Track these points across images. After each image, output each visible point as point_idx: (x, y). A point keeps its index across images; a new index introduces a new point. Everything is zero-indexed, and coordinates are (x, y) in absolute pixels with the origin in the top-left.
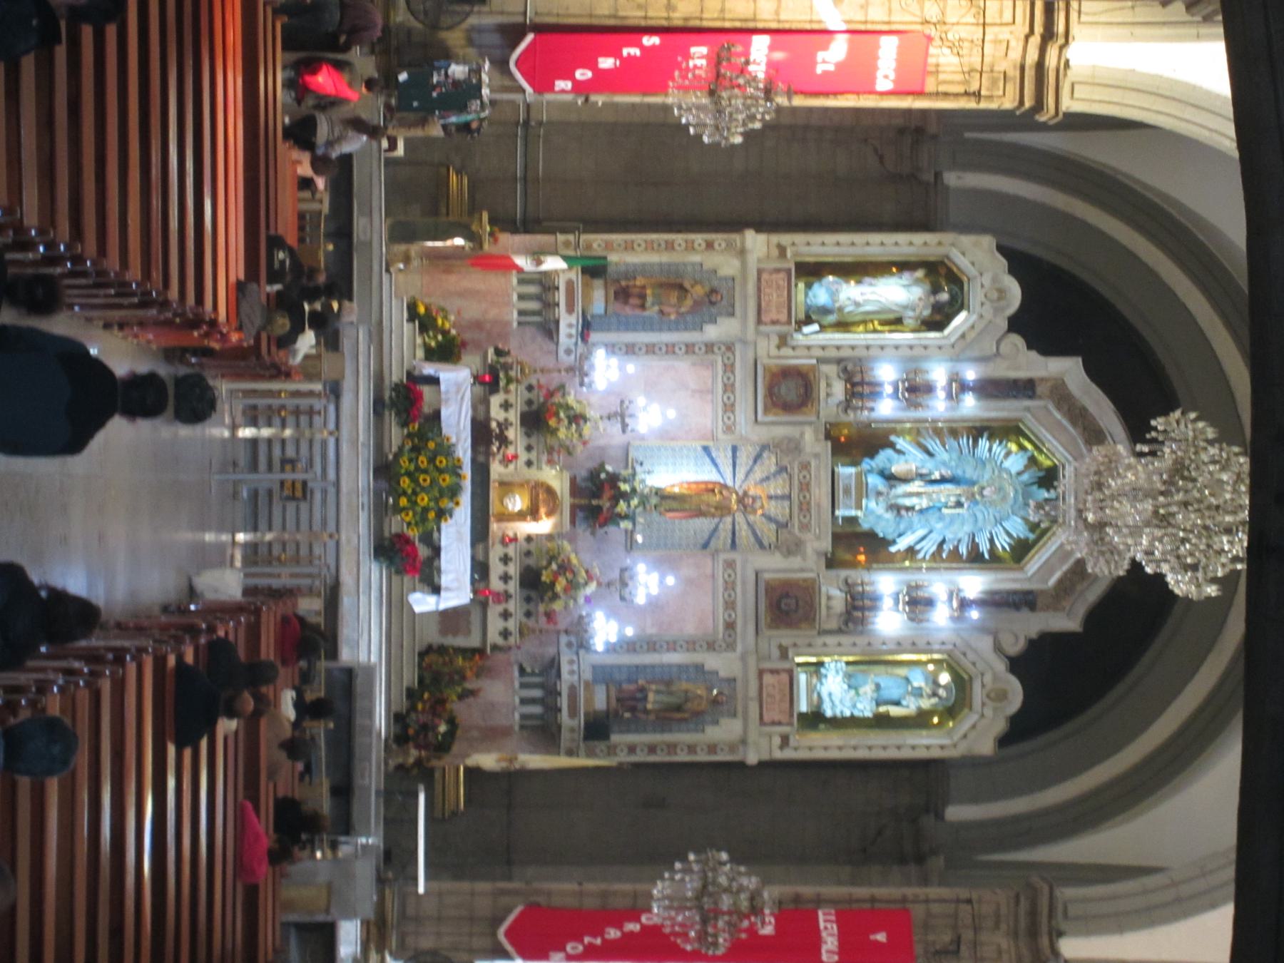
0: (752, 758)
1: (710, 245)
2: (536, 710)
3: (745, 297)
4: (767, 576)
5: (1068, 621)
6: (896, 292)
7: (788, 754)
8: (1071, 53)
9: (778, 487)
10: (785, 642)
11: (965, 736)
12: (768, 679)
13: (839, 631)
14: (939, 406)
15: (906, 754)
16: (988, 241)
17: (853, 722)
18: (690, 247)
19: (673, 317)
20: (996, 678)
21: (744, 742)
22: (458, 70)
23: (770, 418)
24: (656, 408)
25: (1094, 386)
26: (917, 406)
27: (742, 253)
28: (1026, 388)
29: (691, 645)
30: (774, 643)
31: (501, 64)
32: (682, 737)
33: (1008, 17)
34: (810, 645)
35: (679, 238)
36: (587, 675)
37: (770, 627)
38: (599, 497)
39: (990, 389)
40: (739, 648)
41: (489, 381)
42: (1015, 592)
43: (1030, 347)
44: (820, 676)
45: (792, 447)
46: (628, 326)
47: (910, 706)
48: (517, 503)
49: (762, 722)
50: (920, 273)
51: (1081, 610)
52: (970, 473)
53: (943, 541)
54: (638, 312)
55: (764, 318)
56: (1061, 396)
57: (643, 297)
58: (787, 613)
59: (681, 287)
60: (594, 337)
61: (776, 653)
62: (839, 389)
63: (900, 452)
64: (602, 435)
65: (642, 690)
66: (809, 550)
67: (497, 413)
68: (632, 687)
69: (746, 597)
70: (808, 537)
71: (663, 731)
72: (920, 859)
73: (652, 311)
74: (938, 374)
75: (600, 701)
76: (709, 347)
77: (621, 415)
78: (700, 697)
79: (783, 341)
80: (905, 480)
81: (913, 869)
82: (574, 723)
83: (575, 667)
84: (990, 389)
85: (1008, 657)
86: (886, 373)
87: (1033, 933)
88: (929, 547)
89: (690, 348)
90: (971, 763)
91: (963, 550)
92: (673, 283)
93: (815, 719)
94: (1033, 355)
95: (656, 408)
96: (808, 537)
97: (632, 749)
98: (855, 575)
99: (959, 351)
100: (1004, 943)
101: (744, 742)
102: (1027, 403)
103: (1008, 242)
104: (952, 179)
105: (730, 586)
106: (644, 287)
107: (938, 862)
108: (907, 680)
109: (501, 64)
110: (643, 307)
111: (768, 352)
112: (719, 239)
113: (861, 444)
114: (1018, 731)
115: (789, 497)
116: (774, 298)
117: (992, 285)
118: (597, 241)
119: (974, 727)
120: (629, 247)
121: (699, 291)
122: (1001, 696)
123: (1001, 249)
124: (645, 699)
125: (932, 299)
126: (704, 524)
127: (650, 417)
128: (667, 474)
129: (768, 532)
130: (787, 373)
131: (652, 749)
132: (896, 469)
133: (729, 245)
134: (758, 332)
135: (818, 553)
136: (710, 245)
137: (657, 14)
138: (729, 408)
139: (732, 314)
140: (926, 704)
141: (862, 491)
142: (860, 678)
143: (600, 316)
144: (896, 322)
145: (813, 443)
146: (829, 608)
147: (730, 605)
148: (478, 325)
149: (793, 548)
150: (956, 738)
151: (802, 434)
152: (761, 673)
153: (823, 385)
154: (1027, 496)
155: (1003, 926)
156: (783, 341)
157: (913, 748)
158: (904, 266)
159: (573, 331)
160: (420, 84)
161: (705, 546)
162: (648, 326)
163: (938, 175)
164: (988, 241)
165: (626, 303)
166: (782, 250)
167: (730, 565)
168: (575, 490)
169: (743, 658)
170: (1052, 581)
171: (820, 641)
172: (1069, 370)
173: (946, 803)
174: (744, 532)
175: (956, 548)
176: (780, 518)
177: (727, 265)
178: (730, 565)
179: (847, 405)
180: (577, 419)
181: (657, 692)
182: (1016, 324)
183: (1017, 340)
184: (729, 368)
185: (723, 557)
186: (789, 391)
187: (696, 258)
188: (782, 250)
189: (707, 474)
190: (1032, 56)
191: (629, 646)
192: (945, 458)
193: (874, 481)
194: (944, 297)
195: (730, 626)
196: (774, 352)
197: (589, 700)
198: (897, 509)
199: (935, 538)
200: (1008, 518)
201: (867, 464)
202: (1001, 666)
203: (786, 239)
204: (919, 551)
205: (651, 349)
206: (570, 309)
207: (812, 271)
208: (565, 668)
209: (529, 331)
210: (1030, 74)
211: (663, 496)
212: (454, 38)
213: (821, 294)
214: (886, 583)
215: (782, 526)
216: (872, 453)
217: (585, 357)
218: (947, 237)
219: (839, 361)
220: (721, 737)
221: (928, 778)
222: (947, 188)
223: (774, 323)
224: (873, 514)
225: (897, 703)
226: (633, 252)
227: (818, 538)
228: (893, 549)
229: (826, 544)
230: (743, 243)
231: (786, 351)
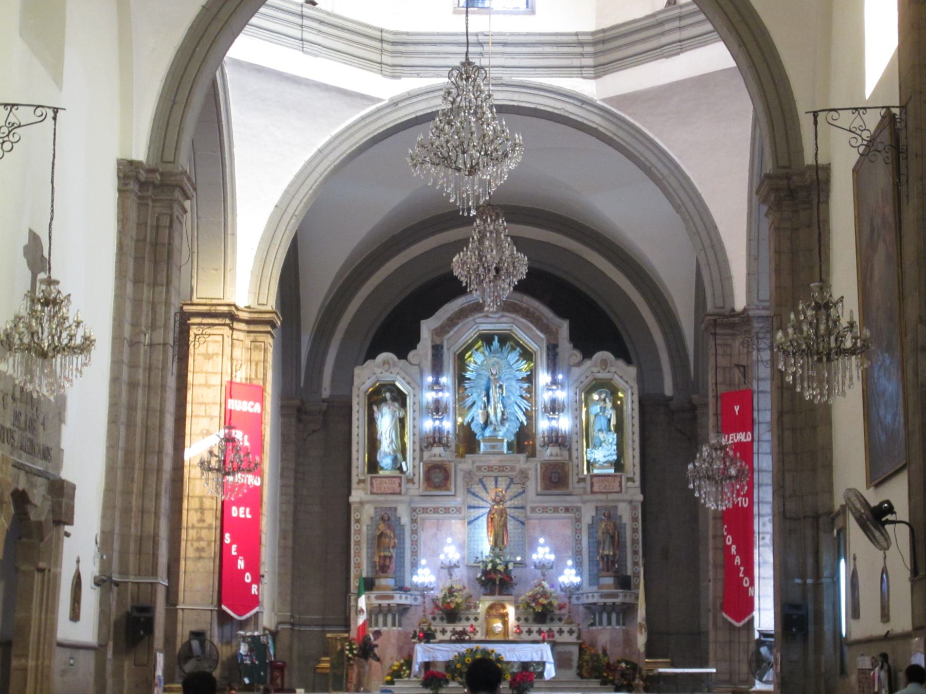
0: (640, 497)
1: (358, 521)
2: (614, 616)
3: (386, 501)
4: (539, 489)
5: (564, 328)
6: (385, 422)
7: (637, 478)
8: (241, 305)
9: (491, 484)
10: (575, 479)
11: (627, 382)
12: (596, 489)
13: (570, 450)
14: (447, 396)
15: (636, 414)
16: (357, 371)
18: (359, 532)
19: (396, 541)
20: (595, 366)
21: (631, 502)
22: (244, 649)
24: (447, 549)
25: (437, 314)
26: (446, 408)
27: (362, 503)
28: (437, 350)
29: (578, 531)
30: (577, 485)
31: (242, 625)
34: (577, 466)
35: (353, 538)
36: (595, 588)
37: (567, 488)
38: (496, 580)
39: (437, 370)
40: (579, 505)
41: (428, 637)
42: (548, 355)
44: (595, 461)
45: (469, 475)
46: (402, 566)
47: (611, 413)
48: (498, 625)
49: (621, 492)
50: (375, 408)
51: (557, 320)
52: (483, 382)
53: (521, 396)
54: (393, 560)
55: (398, 491)
56: (441, 331)
57: (385, 557)
58: (559, 478)
59: (381, 535)
60: (407, 585)
61: (582, 485)
62: (437, 450)
63: (473, 420)
64: (461, 576)
65: (602, 558)
67: (447, 636)
68: (601, 564)
69: (551, 501)
70: (518, 467)
71: (625, 547)
72: (693, 408)
73: (393, 552)
74: (429, 396)
75: (609, 581)
76: (414, 521)
77: (450, 568)
78: (606, 526)
79: (410, 481)
80: (488, 415)
81: (698, 412)
82: (621, 595)
83: (590, 595)
84: (437, 370)
85: (584, 358)
86: (428, 425)
88: (524, 404)
89: (414, 532)
90: (641, 379)
91: (526, 385)
92: (378, 540)
93: (618, 465)
94: (419, 346)
95: (447, 549)
96: (518, 467)
97: (635, 564)
98: (539, 441)
99: (418, 386)
101: (631, 502)
102: (445, 349)
104: (326, 393)
105: (545, 510)
106: (380, 557)
107: (695, 397)
108: (596, 415)
109: (242, 625)
110: (391, 557)
111: (417, 489)
112: (353, 517)
113: (468, 441)
114: (623, 354)
116: (387, 486)
118: (354, 583)
119: (621, 377)
120: (358, 566)
121: (382, 527)
122: (604, 363)
124: (607, 556)
125: (390, 402)
126: (511, 524)
127: (451, 553)
128: (484, 546)
129: (515, 489)
130: (428, 479)
131: (635, 553)
132: (481, 420)
133: (357, 510)
134: (406, 494)
135: (527, 461)
137: (213, 535)
138: (447, 510)
139: (396, 509)
140: (609, 405)
141: (493, 439)
142: (596, 440)
143: (396, 581)
144: (402, 421)
145: (467, 463)
146: (557, 455)
147: (556, 510)
148: (400, 649)
149: (524, 475)
150: (627, 387)
151: (461, 470)
152: (592, 492)
153: (434, 459)
154: (496, 352)
155: (729, 342)
156: (410, 481)
157: (633, 410)
159: (404, 596)
160: (251, 671)
161: (523, 523)
162: (401, 556)
163: (323, 401)
165: (388, 567)
166: (360, 481)
167: (533, 510)
168: (492, 593)
169: (584, 502)
170: (542, 336)
171: (575, 460)
172: (427, 327)
173: (663, 395)
174: (516, 502)
175: (525, 389)
176: (508, 482)
177: (368, 512)
178: (533, 510)
179: (446, 446)
180: (451, 591)
181: (603, 549)
182: (402, 354)
183: (411, 355)
184: (425, 510)
185: (529, 514)
186: (437, 477)
187: (364, 528)
188: (361, 481)
189: (483, 522)
190: (243, 326)
191: (578, 565)
192: (476, 395)
193: (488, 433)
194: (388, 395)
195: (567, 510)
196: (416, 486)
197: (608, 587)
198: (503, 420)
199: (519, 400)
200: (509, 362)
201: (479, 437)
202: (588, 363)
203: (354, 479)
204: (526, 409)
205: (415, 553)
206: (392, 597)
207: (373, 466)
208: (591, 600)
209: (405, 621)
211: (495, 545)
212: (225, 652)
213: (385, 461)
214: (543, 425)
216: (474, 435)
217: (416, 587)
218: (355, 392)
219: (422, 450)
221: (650, 405)
222: (330, 396)
223: (400, 485)
224: (506, 433)
225: (609, 420)
227: (519, 461)
228: (525, 423)
229: (522, 457)
230: (356, 503)
231: (416, 480)
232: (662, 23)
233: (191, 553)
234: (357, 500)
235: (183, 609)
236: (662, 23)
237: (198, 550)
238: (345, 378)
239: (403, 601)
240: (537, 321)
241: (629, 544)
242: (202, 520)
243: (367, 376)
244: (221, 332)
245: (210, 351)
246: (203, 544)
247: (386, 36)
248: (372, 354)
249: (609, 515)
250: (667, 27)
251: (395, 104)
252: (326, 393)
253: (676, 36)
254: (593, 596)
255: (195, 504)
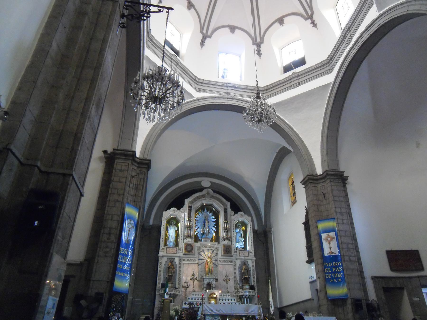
0: (255, 259)
2: (248, 300)
4: (222, 254)
5: (229, 204)
7: (253, 252)
12: (240, 255)
16: (164, 213)
17: (245, 241)
18: (161, 267)
21: (252, 260)
23: (193, 252)
27: (163, 256)
29: (235, 269)
32: (252, 272)
33: (127, 164)
35: (159, 269)
37: (231, 254)
42: (224, 212)
43: (183, 207)
45: (199, 248)
50: (168, 226)
56: (192, 202)
59: (169, 268)
60: (177, 287)
61: (236, 253)
62: (189, 239)
66: (218, 246)
69: (227, 258)
76: (180, 264)
80: (204, 231)
87: (317, 180)
89: (180, 267)
96: (215, 246)
97: (254, 281)
100: (320, 185)
101: (252, 260)
102: (192, 208)
103: (165, 209)
104: (151, 223)
105: (224, 261)
112: (159, 261)
115: (208, 250)
117: (172, 212)
118: (158, 286)
120: (160, 279)
121: (170, 264)
123: (166, 211)
129: (214, 254)
136: (161, 263)
138: (192, 260)
147: (227, 262)
155: (316, 186)
158: (167, 229)
163: (150, 225)
164: (164, 213)
167: (220, 261)
169: (236, 259)
172: (187, 202)
177: (165, 260)
178: (220, 261)
182: (179, 209)
183: (181, 209)
187: (163, 265)
190: (136, 164)
195: (231, 262)
196: (181, 251)
201: (200, 238)
202: (236, 215)
203: (161, 248)
210: (140, 166)
215: (213, 251)
219: (184, 240)
220: (251, 264)
225: (241, 234)
226: (161, 279)
232: (290, 79)
233: (101, 254)
234: (162, 255)
235: (93, 280)
236: (290, 79)
237: (106, 252)
238: (159, 217)
239: (176, 293)
240: (221, 202)
241: (252, 274)
242: (109, 239)
243: (167, 214)
244: (128, 162)
245: (123, 168)
246: (108, 250)
247: (197, 79)
248: (169, 208)
249: (244, 263)
250: (292, 80)
251: (198, 100)
252: (151, 223)
253: (297, 81)
254: (242, 292)
255: (107, 231)
